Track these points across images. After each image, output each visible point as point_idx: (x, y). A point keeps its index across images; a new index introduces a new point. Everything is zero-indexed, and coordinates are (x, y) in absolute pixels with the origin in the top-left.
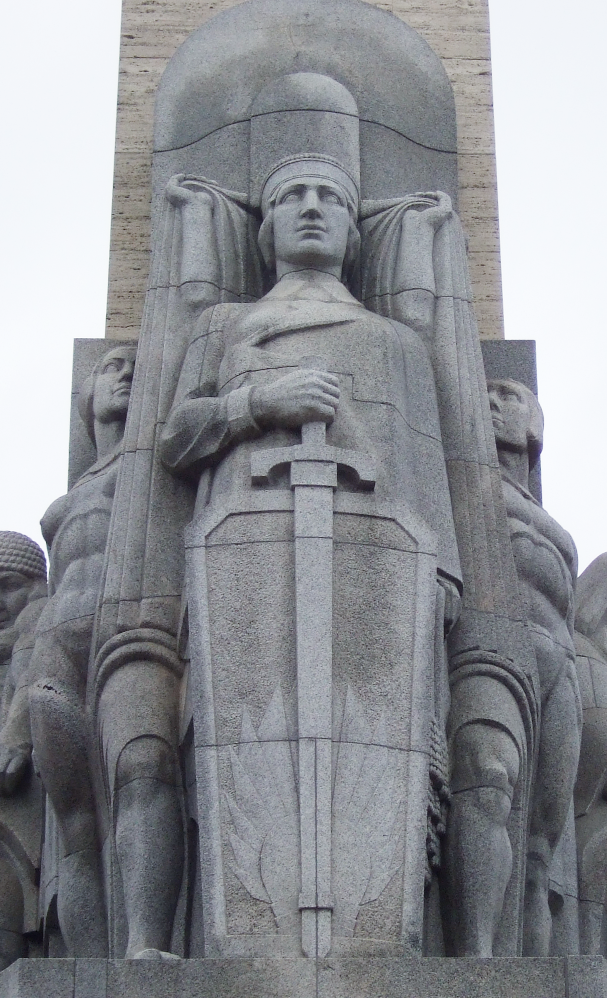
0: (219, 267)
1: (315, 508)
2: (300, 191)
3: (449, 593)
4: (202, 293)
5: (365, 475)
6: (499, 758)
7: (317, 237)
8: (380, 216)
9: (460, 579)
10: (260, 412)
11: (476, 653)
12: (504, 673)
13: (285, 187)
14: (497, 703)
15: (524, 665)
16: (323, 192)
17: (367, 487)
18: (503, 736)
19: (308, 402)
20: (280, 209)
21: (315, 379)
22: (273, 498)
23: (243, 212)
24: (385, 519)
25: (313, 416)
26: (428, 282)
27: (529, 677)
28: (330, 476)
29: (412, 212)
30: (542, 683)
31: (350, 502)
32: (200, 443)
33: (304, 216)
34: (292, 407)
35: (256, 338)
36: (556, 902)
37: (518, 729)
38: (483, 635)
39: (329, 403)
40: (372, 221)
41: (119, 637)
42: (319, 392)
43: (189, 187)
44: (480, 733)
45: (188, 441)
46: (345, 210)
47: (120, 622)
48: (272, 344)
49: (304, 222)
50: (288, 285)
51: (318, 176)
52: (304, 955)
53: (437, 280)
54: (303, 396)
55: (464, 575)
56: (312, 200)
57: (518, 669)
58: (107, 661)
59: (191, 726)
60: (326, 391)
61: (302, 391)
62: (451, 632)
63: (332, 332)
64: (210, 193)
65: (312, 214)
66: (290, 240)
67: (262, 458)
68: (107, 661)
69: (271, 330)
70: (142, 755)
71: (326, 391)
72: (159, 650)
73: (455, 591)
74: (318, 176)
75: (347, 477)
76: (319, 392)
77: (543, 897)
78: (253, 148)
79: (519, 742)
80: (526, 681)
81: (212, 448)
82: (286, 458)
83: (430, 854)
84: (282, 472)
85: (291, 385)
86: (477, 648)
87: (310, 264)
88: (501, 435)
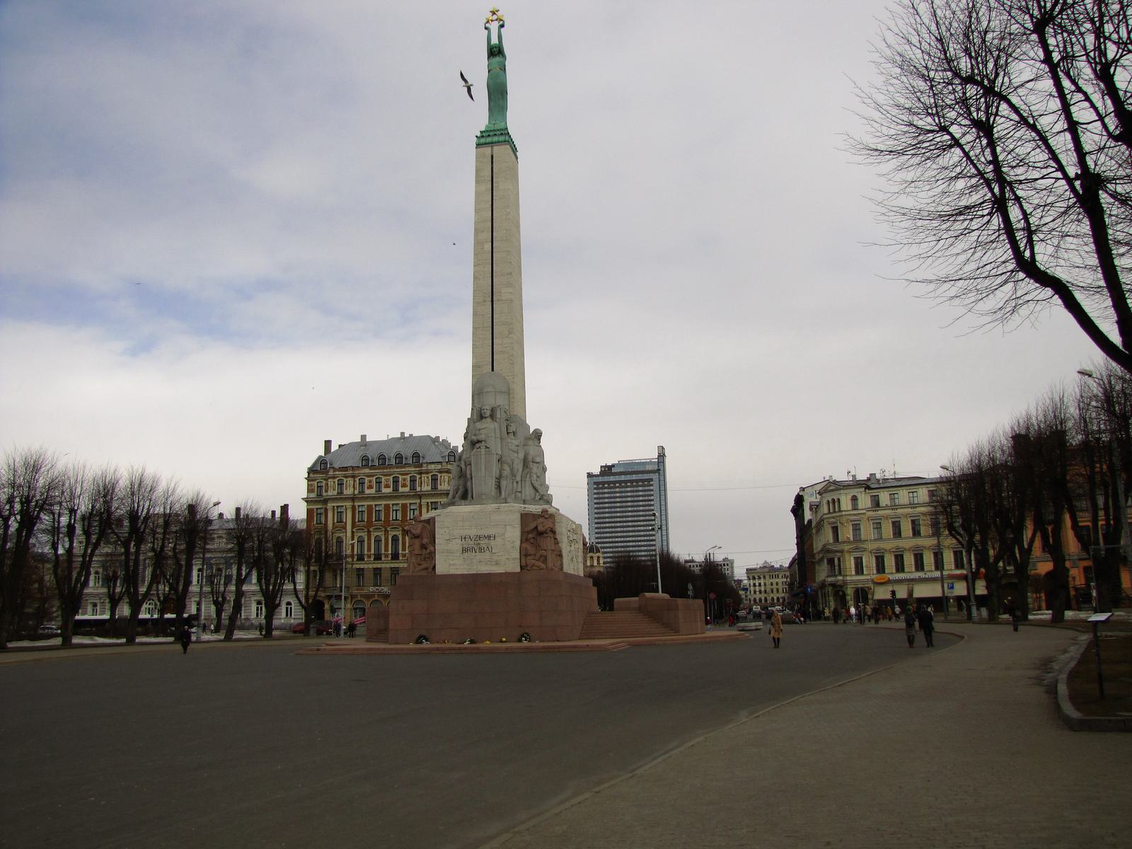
1: (483, 451)
22: (479, 450)
31: (487, 450)
36: (517, 482)
67: (478, 445)
77: (515, 483)
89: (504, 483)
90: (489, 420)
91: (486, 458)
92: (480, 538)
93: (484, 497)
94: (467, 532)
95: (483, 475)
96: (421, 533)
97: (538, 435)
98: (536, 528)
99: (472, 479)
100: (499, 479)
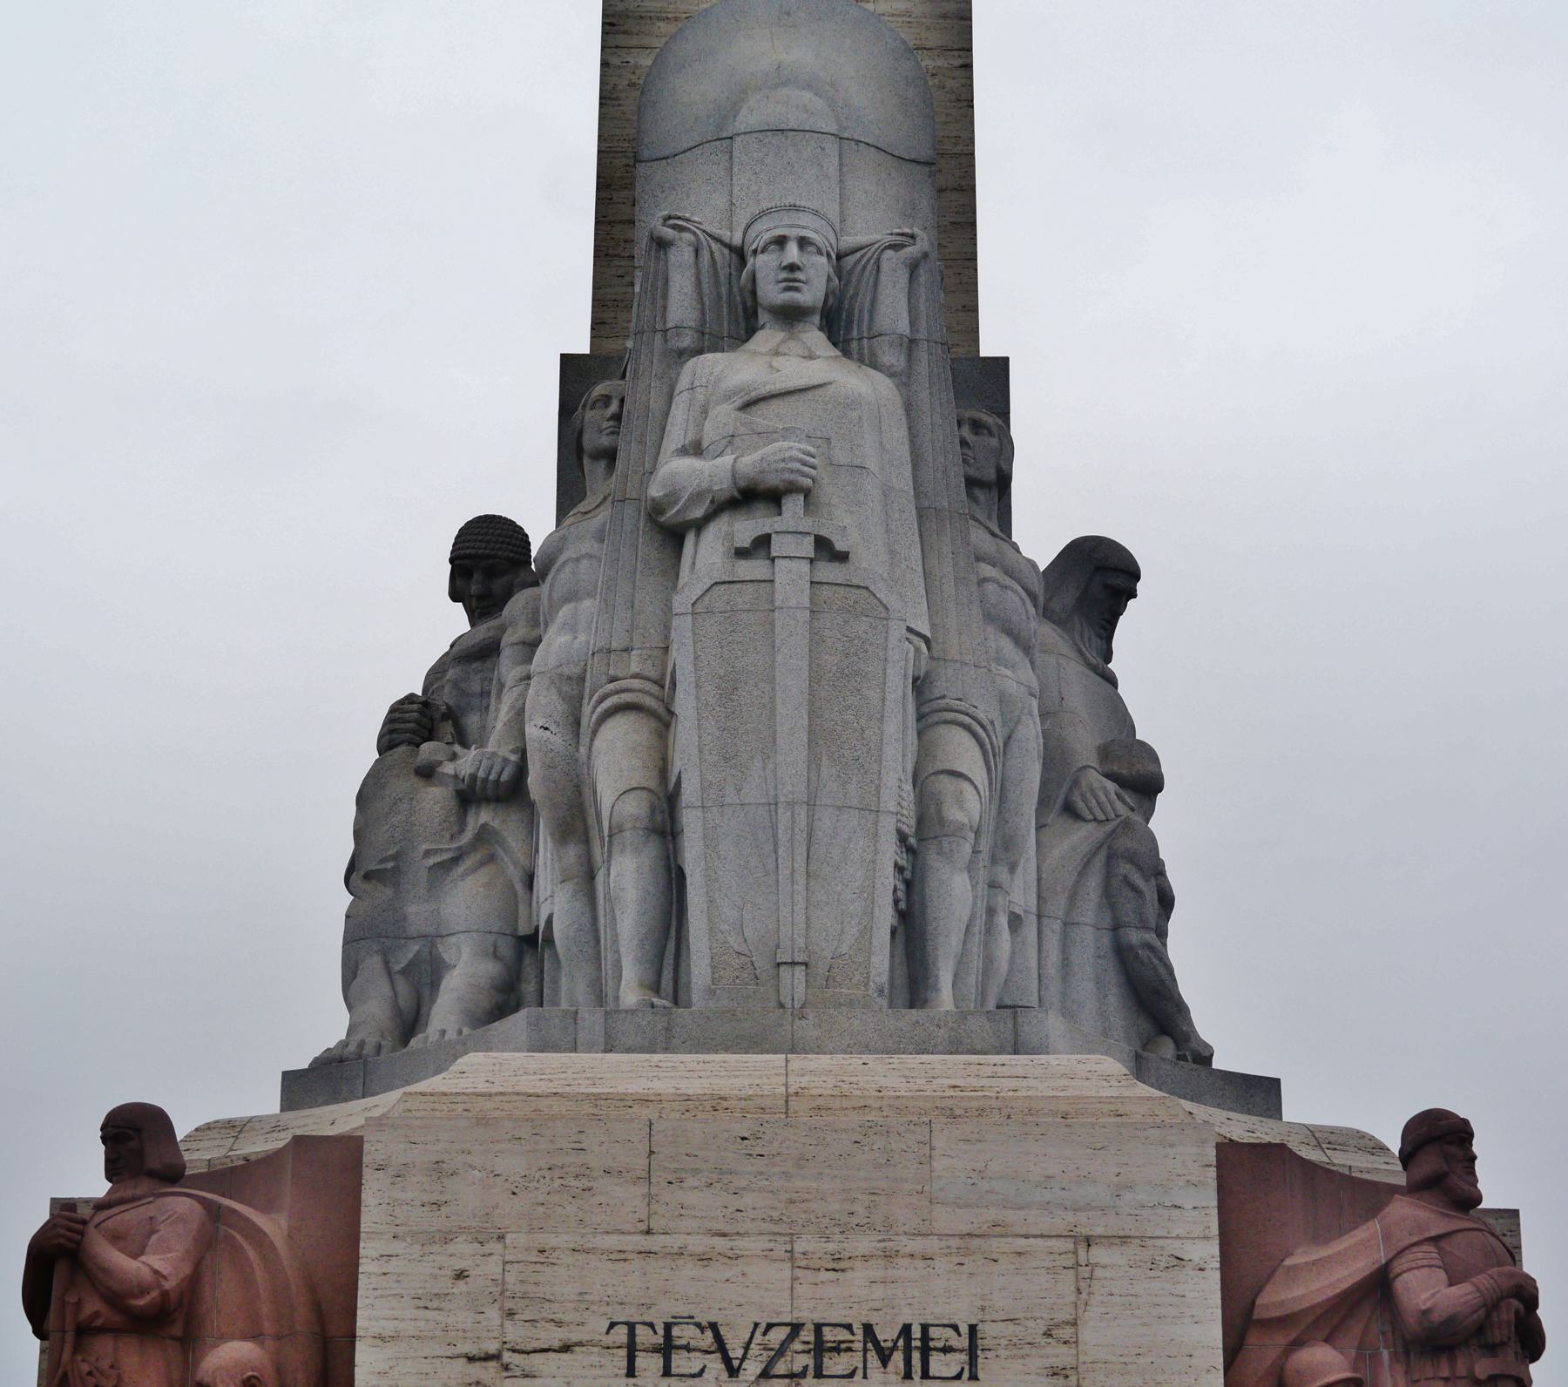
0: (703, 313)
1: (791, 575)
2: (781, 242)
3: (917, 650)
4: (686, 341)
5: (840, 546)
6: (961, 808)
7: (797, 289)
8: (859, 254)
9: (928, 634)
10: (742, 484)
11: (942, 703)
12: (967, 720)
13: (767, 236)
14: (961, 751)
15: (986, 710)
16: (803, 243)
17: (843, 557)
18: (966, 785)
19: (787, 476)
20: (761, 258)
21: (795, 453)
22: (753, 568)
23: (726, 251)
24: (859, 587)
25: (793, 488)
26: (904, 326)
27: (992, 723)
28: (807, 547)
29: (890, 253)
30: (1004, 724)
31: (829, 571)
32: (686, 507)
33: (785, 268)
34: (773, 480)
35: (739, 402)
36: (1015, 922)
37: (979, 775)
38: (947, 686)
39: (807, 476)
40: (851, 260)
41: (611, 686)
42: (798, 466)
43: (674, 227)
44: (946, 785)
45: (675, 503)
46: (824, 260)
47: (612, 672)
48: (754, 408)
49: (784, 275)
50: (768, 337)
51: (798, 226)
52: (782, 1006)
53: (912, 323)
54: (784, 470)
55: (933, 626)
56: (792, 253)
57: (981, 716)
58: (599, 710)
59: (679, 778)
60: (804, 464)
61: (782, 465)
62: (920, 685)
63: (810, 395)
64: (694, 233)
65: (792, 268)
66: (771, 292)
67: (745, 528)
68: (599, 710)
69: (753, 394)
70: (635, 807)
71: (804, 464)
72: (649, 701)
73: (923, 647)
74: (798, 226)
75: (823, 546)
76: (798, 466)
77: (1002, 920)
78: (735, 169)
79: (980, 787)
80: (989, 727)
81: (698, 513)
82: (767, 530)
83: (896, 902)
84: (763, 542)
85: (771, 458)
86: (944, 697)
87: (790, 316)
88: (972, 472)
89: (955, 893)
90: (814, 337)
91: (816, 640)
92: (820, 1349)
93: (794, 984)
94: (684, 1292)
95: (793, 782)
96: (193, 1283)
97: (1099, 580)
98: (1379, 1286)
99: (665, 827)
100: (919, 844)
